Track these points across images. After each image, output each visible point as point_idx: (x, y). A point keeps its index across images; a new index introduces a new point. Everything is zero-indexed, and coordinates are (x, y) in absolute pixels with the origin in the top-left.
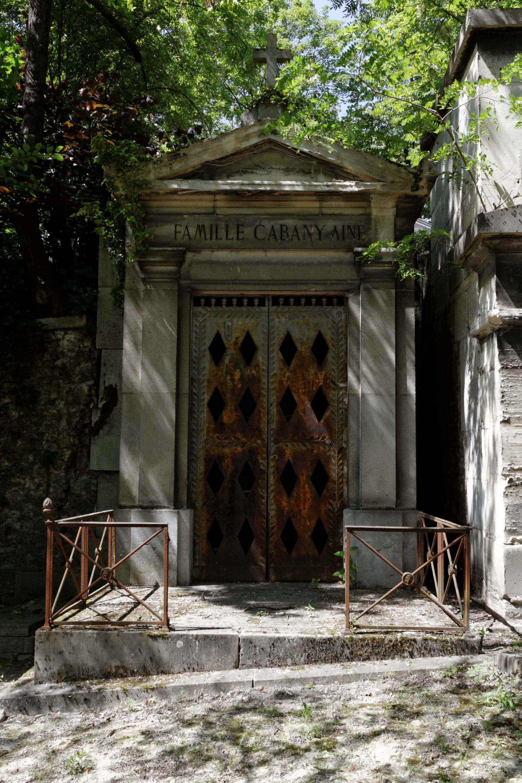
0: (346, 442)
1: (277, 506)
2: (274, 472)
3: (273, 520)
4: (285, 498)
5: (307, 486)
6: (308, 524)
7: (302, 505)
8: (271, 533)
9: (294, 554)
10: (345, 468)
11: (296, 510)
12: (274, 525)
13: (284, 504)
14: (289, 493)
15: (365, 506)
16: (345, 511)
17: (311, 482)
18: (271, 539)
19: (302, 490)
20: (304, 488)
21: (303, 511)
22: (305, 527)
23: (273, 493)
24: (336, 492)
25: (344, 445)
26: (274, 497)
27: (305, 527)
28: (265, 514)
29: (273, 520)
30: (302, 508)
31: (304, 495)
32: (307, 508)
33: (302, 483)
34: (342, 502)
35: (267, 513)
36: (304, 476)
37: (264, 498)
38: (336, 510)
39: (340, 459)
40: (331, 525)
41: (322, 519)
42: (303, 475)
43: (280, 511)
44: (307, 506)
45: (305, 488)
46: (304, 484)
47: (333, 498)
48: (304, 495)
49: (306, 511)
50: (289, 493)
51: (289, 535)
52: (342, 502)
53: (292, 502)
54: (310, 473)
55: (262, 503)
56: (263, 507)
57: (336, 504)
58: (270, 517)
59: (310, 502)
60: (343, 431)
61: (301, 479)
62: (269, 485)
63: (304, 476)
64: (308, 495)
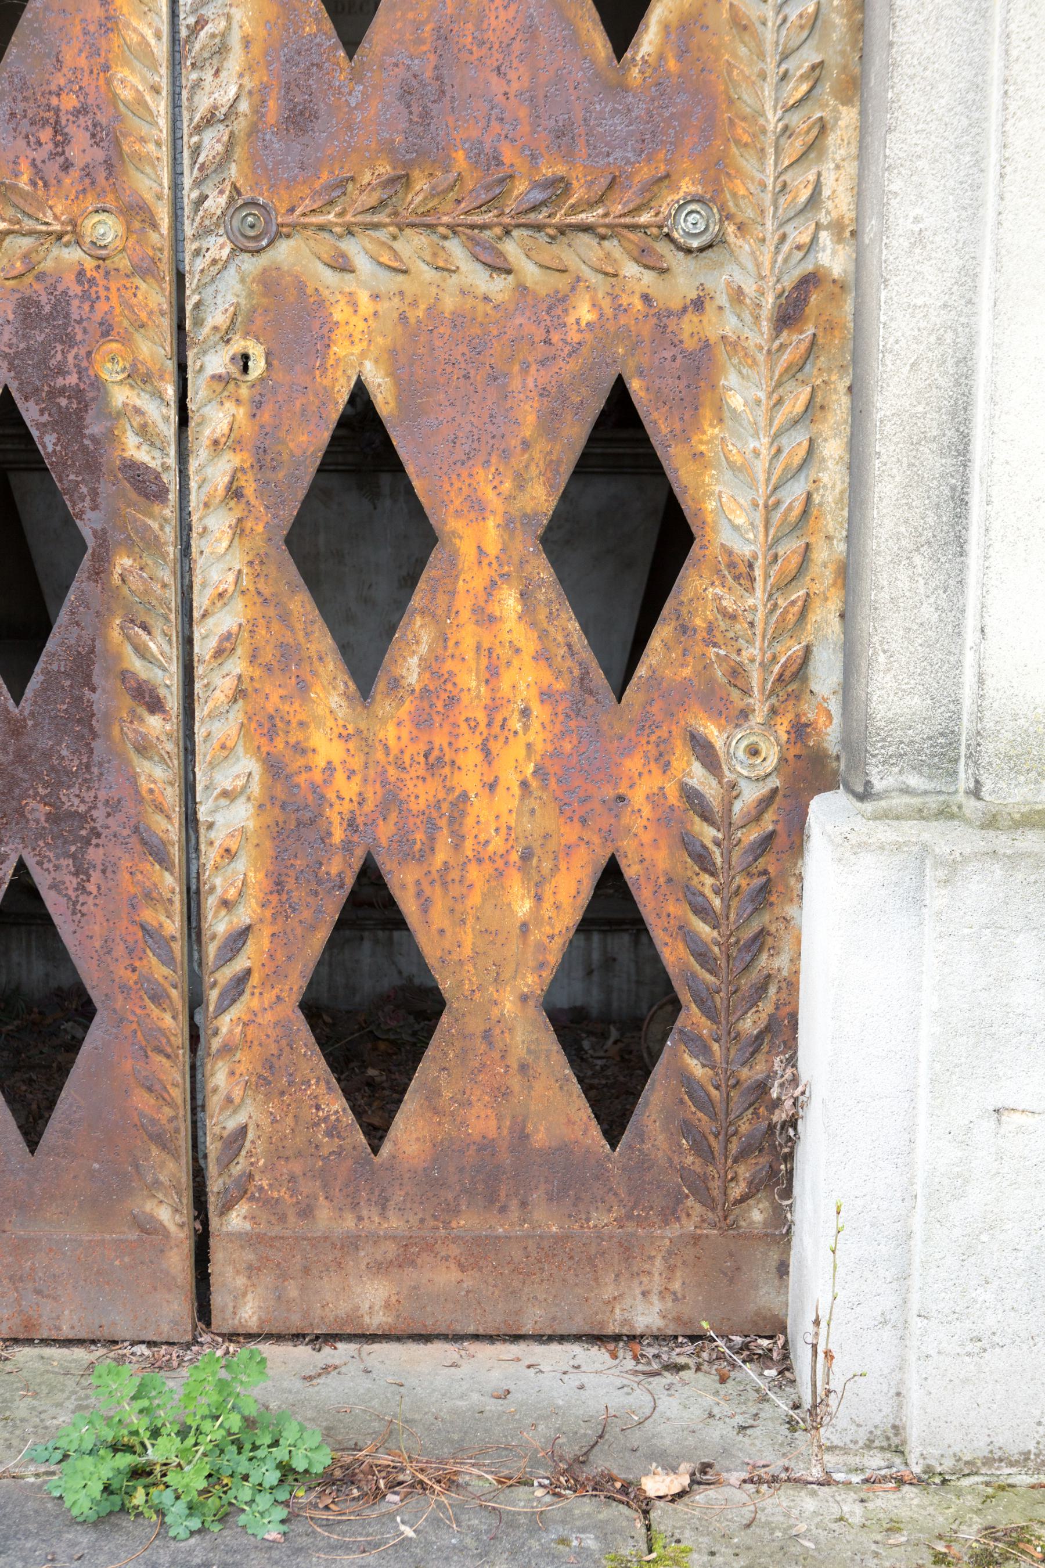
0: (850, 233)
1: (274, 767)
2: (234, 492)
3: (236, 880)
4: (331, 694)
5: (509, 602)
6: (523, 907)
7: (471, 758)
8: (226, 974)
9: (410, 1131)
10: (833, 449)
11: (421, 794)
12: (244, 915)
13: (326, 748)
14: (365, 664)
15: (1013, 794)
16: (827, 814)
17: (543, 571)
18: (226, 1023)
19: (468, 636)
20: (487, 619)
21: (479, 808)
22: (497, 944)
23: (237, 665)
24: (752, 652)
25: (833, 259)
26: (239, 694)
27: (497, 944)
28: (169, 829)
29: (236, 880)
30: (469, 781)
31: (492, 674)
32: (510, 779)
33: (472, 580)
34: (800, 730)
35: (190, 820)
36: (491, 507)
37: (155, 706)
38: (750, 794)
39: (796, 370)
40: (703, 911)
41: (631, 871)
42: (478, 508)
43: (293, 816)
44: (514, 763)
45: (493, 608)
46: (491, 587)
47: (724, 695)
48: (492, 674)
49: (507, 800)
50: (365, 664)
51: (373, 1018)
52: (800, 730)
53: (389, 733)
54: (541, 499)
55: (144, 749)
56: (157, 776)
57: (750, 758)
58: (210, 856)
59: (536, 735)
60: (823, 128)
61: (466, 549)
62: (201, 601)
63: (491, 507)
64: (524, 680)
